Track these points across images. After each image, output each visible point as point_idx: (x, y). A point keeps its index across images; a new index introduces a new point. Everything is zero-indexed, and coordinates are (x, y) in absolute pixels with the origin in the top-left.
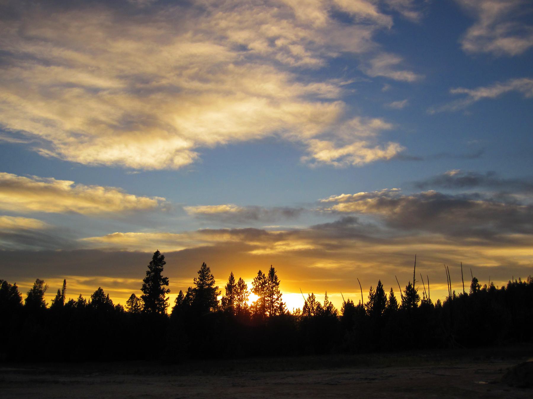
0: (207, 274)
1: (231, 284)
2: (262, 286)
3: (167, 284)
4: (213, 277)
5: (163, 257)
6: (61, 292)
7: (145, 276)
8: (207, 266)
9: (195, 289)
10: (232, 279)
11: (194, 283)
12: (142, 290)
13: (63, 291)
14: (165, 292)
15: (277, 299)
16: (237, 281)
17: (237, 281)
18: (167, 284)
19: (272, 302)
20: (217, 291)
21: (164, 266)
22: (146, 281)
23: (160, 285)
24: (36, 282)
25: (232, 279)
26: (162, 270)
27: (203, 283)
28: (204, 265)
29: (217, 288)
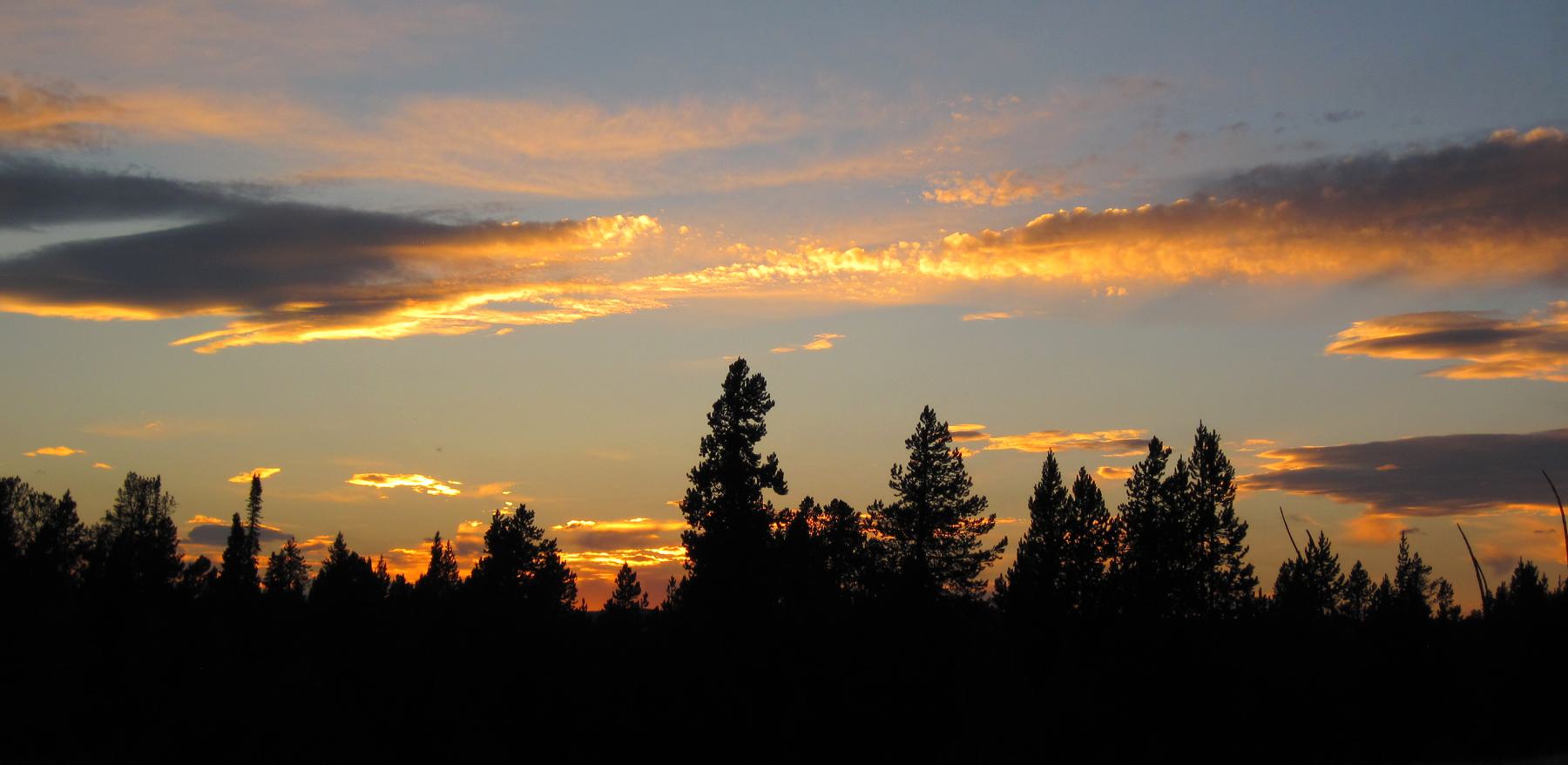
0: (937, 447)
1: (1051, 488)
3: (781, 489)
4: (960, 459)
5: (759, 381)
6: (245, 522)
7: (697, 460)
8: (940, 419)
9: (895, 507)
10: (1051, 469)
11: (893, 485)
12: (684, 509)
13: (253, 519)
15: (1233, 547)
16: (1068, 480)
17: (1068, 480)
18: (781, 489)
19: (1214, 559)
20: (983, 516)
21: (769, 418)
22: (702, 476)
23: (757, 494)
24: (127, 483)
25: (1051, 469)
26: (757, 434)
28: (928, 415)
29: (977, 504)
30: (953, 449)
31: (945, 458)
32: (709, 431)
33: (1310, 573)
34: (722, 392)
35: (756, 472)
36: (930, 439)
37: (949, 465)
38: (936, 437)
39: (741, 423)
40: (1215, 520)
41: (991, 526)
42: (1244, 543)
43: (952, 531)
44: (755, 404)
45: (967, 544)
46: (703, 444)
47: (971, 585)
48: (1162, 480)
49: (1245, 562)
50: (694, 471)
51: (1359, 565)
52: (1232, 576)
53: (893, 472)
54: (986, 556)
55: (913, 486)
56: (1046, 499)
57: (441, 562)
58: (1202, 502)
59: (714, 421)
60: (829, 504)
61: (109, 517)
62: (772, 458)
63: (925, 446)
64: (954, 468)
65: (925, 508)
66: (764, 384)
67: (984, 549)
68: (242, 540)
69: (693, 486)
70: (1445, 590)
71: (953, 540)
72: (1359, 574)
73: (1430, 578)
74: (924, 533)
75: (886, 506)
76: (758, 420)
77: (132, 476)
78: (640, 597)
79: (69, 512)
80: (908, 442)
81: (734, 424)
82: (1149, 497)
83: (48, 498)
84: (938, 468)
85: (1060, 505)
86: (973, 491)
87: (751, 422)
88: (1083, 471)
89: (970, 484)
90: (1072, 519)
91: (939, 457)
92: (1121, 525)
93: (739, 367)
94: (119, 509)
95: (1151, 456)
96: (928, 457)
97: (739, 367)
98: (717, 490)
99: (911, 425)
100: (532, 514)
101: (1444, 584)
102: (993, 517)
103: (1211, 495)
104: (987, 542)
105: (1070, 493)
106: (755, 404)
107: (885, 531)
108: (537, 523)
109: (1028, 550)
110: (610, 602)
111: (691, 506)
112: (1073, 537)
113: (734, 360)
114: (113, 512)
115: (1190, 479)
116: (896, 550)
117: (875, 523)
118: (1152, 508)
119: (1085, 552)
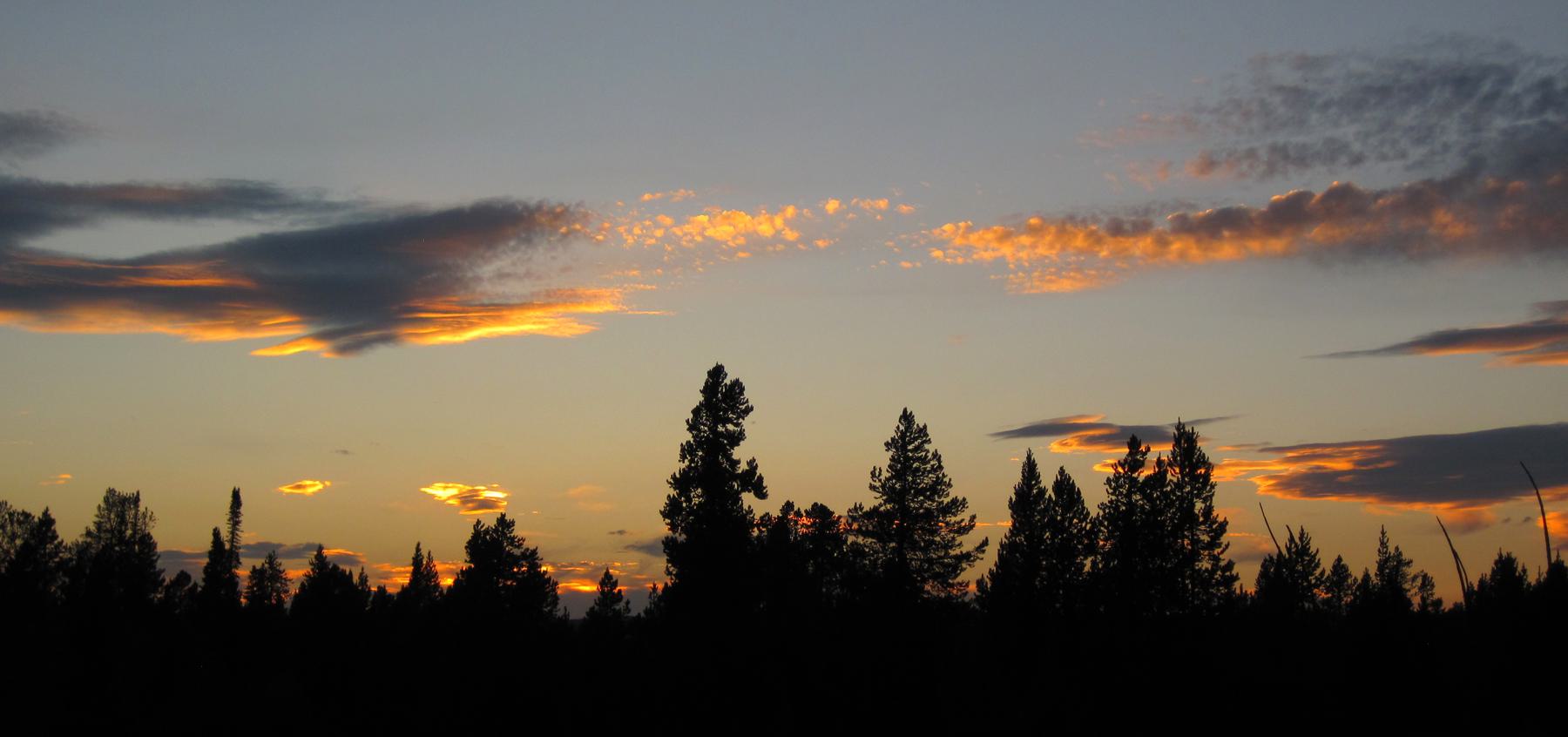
0: (916, 449)
1: (1031, 488)
2: (1145, 496)
3: (761, 493)
5: (737, 387)
6: (225, 534)
7: (676, 466)
8: (919, 421)
9: (875, 510)
10: (1030, 469)
11: (872, 488)
12: (665, 514)
13: (233, 533)
14: (753, 526)
15: (1214, 543)
16: (1047, 480)
17: (1047, 480)
18: (761, 493)
19: (1194, 556)
20: (964, 516)
21: (746, 423)
22: (681, 483)
24: (106, 500)
25: (1030, 469)
26: (736, 439)
27: (904, 491)
28: (907, 417)
29: (957, 505)
30: (932, 451)
31: (924, 460)
32: (689, 437)
33: (1290, 567)
34: (700, 398)
35: (736, 477)
36: (909, 441)
37: (928, 467)
38: (915, 439)
39: (720, 428)
40: (1194, 517)
41: (972, 527)
42: (1224, 539)
43: (934, 532)
44: (733, 409)
45: (948, 545)
46: (683, 450)
47: (952, 586)
48: (1141, 478)
49: (1225, 558)
50: (674, 477)
51: (1339, 559)
52: (1212, 572)
53: (873, 474)
54: (967, 557)
55: (892, 488)
56: (1026, 499)
57: (422, 571)
58: (1182, 499)
59: (692, 427)
60: (809, 507)
61: (89, 533)
62: (752, 465)
63: (904, 447)
64: (933, 470)
65: (904, 512)
66: (742, 389)
67: (964, 550)
68: (222, 555)
69: (673, 492)
70: (1427, 583)
71: (933, 542)
72: (1340, 568)
73: (1411, 571)
74: (904, 536)
75: (866, 508)
76: (737, 425)
77: (111, 492)
78: (622, 605)
79: (49, 529)
80: (887, 444)
81: (713, 430)
82: (1128, 495)
83: (27, 515)
84: (917, 469)
85: (1040, 507)
86: (954, 493)
87: (730, 427)
88: (1062, 471)
89: (950, 485)
90: (1053, 519)
91: (918, 459)
92: (1101, 524)
93: (717, 373)
94: (99, 525)
95: (1130, 454)
96: (907, 459)
97: (717, 373)
98: (697, 496)
99: (890, 428)
100: (513, 523)
101: (1425, 577)
102: (973, 517)
103: (1190, 492)
104: (968, 543)
105: (1050, 492)
106: (733, 409)
107: (866, 534)
108: (518, 532)
109: (1009, 551)
110: (592, 609)
111: (672, 511)
112: (1053, 536)
113: (711, 366)
114: (93, 528)
115: (1169, 476)
116: (876, 552)
117: (855, 526)
118: (1131, 506)
119: (1067, 551)
